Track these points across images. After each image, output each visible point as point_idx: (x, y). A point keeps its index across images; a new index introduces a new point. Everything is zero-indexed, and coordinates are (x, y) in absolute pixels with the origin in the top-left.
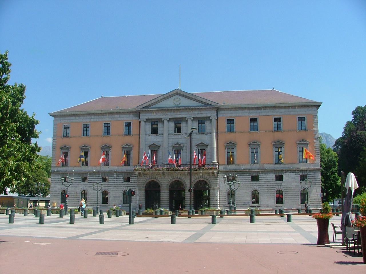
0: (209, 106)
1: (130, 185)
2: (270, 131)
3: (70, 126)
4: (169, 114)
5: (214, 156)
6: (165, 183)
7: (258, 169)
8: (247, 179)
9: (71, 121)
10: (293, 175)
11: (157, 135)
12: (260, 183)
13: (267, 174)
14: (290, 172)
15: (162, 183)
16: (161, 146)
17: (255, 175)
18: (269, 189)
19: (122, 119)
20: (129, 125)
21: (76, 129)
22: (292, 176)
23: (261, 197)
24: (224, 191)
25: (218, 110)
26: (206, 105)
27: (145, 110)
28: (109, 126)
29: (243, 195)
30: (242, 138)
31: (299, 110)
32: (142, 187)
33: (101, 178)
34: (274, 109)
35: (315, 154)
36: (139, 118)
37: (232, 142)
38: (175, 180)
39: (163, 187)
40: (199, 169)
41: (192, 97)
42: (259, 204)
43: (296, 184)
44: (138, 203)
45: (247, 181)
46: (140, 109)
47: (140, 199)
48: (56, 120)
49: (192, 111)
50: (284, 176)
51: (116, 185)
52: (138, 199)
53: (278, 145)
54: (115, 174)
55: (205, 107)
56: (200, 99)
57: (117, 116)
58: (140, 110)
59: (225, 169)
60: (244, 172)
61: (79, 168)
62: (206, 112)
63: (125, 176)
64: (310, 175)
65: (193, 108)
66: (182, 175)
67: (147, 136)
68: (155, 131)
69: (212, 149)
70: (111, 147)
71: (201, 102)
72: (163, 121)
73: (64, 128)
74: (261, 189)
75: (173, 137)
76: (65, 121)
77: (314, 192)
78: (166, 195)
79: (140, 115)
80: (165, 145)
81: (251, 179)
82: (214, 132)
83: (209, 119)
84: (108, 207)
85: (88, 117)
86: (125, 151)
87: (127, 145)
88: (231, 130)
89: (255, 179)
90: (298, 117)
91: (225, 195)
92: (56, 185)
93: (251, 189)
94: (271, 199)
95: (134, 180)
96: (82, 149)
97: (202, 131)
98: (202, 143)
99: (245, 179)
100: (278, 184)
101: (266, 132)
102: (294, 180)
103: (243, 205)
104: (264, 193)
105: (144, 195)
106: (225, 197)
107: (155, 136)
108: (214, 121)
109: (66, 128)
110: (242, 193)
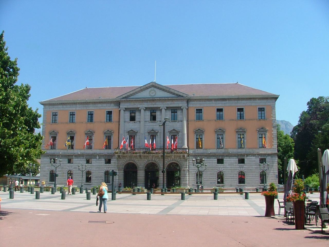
0: (181, 97)
1: (110, 167)
2: (234, 120)
3: (58, 114)
4: (146, 104)
5: (185, 141)
6: (141, 164)
7: (223, 153)
8: (213, 161)
9: (59, 109)
10: (253, 158)
11: (134, 122)
12: (225, 165)
13: (230, 158)
14: (251, 156)
15: (139, 165)
16: (138, 132)
17: (220, 158)
18: (232, 170)
19: (104, 108)
20: (110, 113)
21: (63, 116)
22: (253, 159)
23: (226, 178)
24: (193, 172)
26: (179, 97)
27: (125, 101)
28: (93, 114)
29: (210, 176)
30: (209, 125)
31: (260, 101)
32: (121, 168)
33: (85, 159)
34: (237, 101)
35: (273, 140)
36: (119, 107)
37: (200, 129)
38: (150, 162)
39: (139, 168)
40: (172, 153)
41: (166, 89)
42: (223, 184)
43: (256, 166)
44: (117, 182)
45: (214, 163)
46: (120, 99)
48: (46, 108)
49: (166, 102)
50: (245, 159)
51: (99, 166)
52: (118, 179)
53: (241, 132)
54: (97, 156)
55: (177, 98)
56: (173, 91)
57: (100, 105)
58: (120, 101)
59: (194, 153)
60: (210, 156)
61: (65, 151)
62: (178, 102)
63: (106, 158)
64: (268, 159)
65: (167, 99)
66: (156, 158)
67: (126, 123)
68: (133, 119)
69: (183, 135)
70: (94, 133)
71: (174, 94)
72: (140, 110)
73: (53, 115)
74: (226, 170)
75: (149, 124)
76: (53, 109)
77: (271, 173)
78: (142, 175)
79: (120, 105)
80: (142, 131)
81: (217, 161)
82: (185, 120)
83: (180, 108)
84: (91, 185)
85: (74, 106)
86: (106, 136)
87: (108, 131)
88: (199, 118)
89: (220, 161)
90: (259, 108)
91: (194, 176)
92: (45, 166)
93: (217, 171)
94: (235, 179)
95: (114, 161)
96: (68, 134)
97: (174, 119)
98: (174, 130)
99: (211, 161)
100: (241, 167)
101: (230, 120)
102: (255, 163)
103: (209, 185)
104: (228, 174)
105: (123, 175)
106: (194, 178)
107: (133, 123)
108: (185, 111)
109: (55, 115)
110: (209, 174)
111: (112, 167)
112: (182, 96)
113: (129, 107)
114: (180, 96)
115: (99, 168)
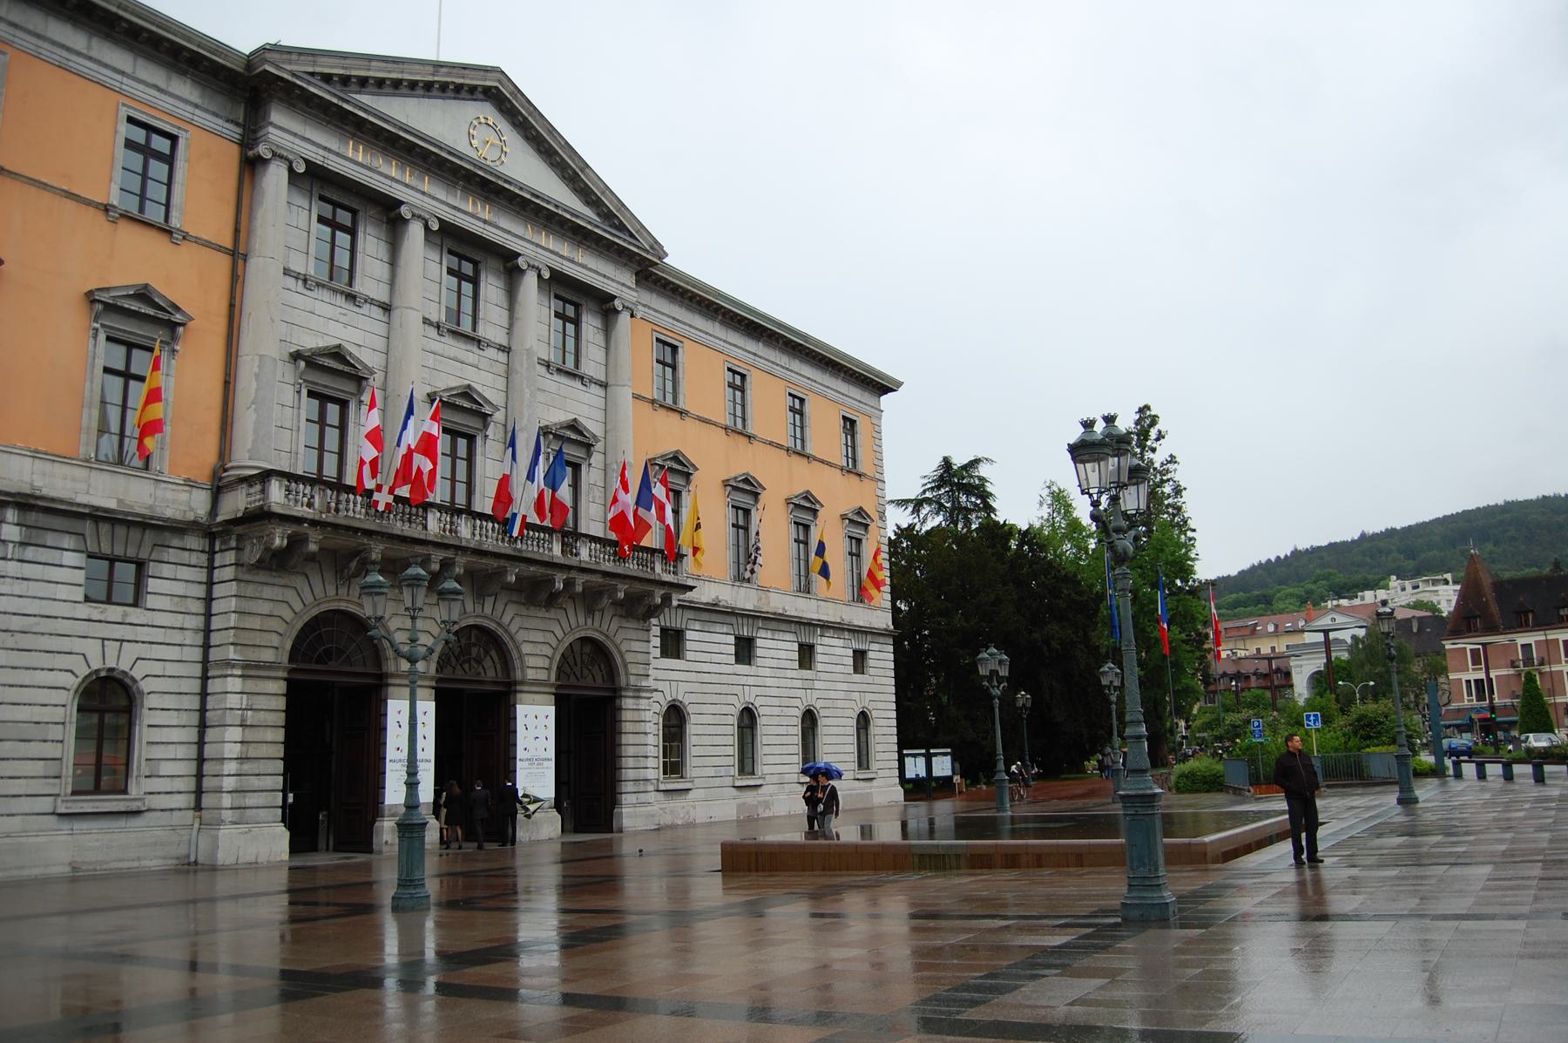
1: (143, 634)
12: (761, 672)
25: (649, 270)
26: (609, 231)
43: (845, 686)
47: (253, 751)
60: (714, 617)
81: (732, 649)
93: (733, 699)
95: (179, 588)
111: (158, 635)
112: (632, 235)
113: (335, 165)
114: (621, 227)
115: (25, 641)
